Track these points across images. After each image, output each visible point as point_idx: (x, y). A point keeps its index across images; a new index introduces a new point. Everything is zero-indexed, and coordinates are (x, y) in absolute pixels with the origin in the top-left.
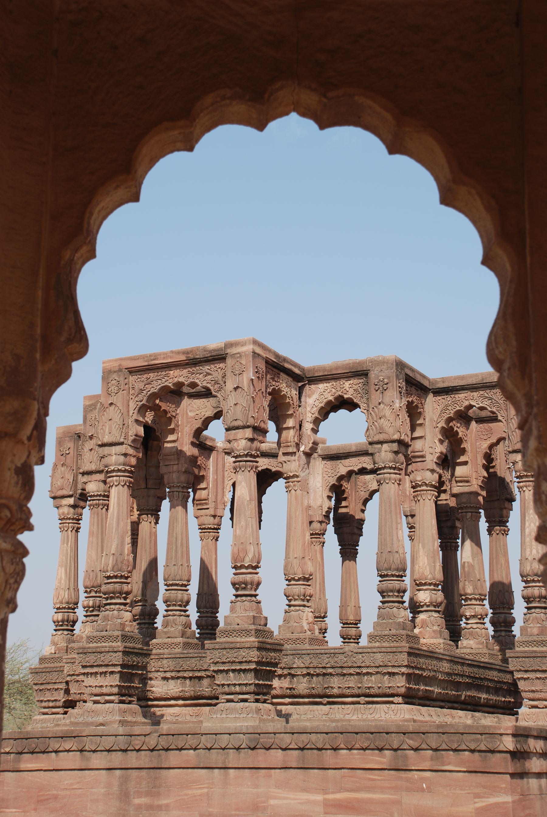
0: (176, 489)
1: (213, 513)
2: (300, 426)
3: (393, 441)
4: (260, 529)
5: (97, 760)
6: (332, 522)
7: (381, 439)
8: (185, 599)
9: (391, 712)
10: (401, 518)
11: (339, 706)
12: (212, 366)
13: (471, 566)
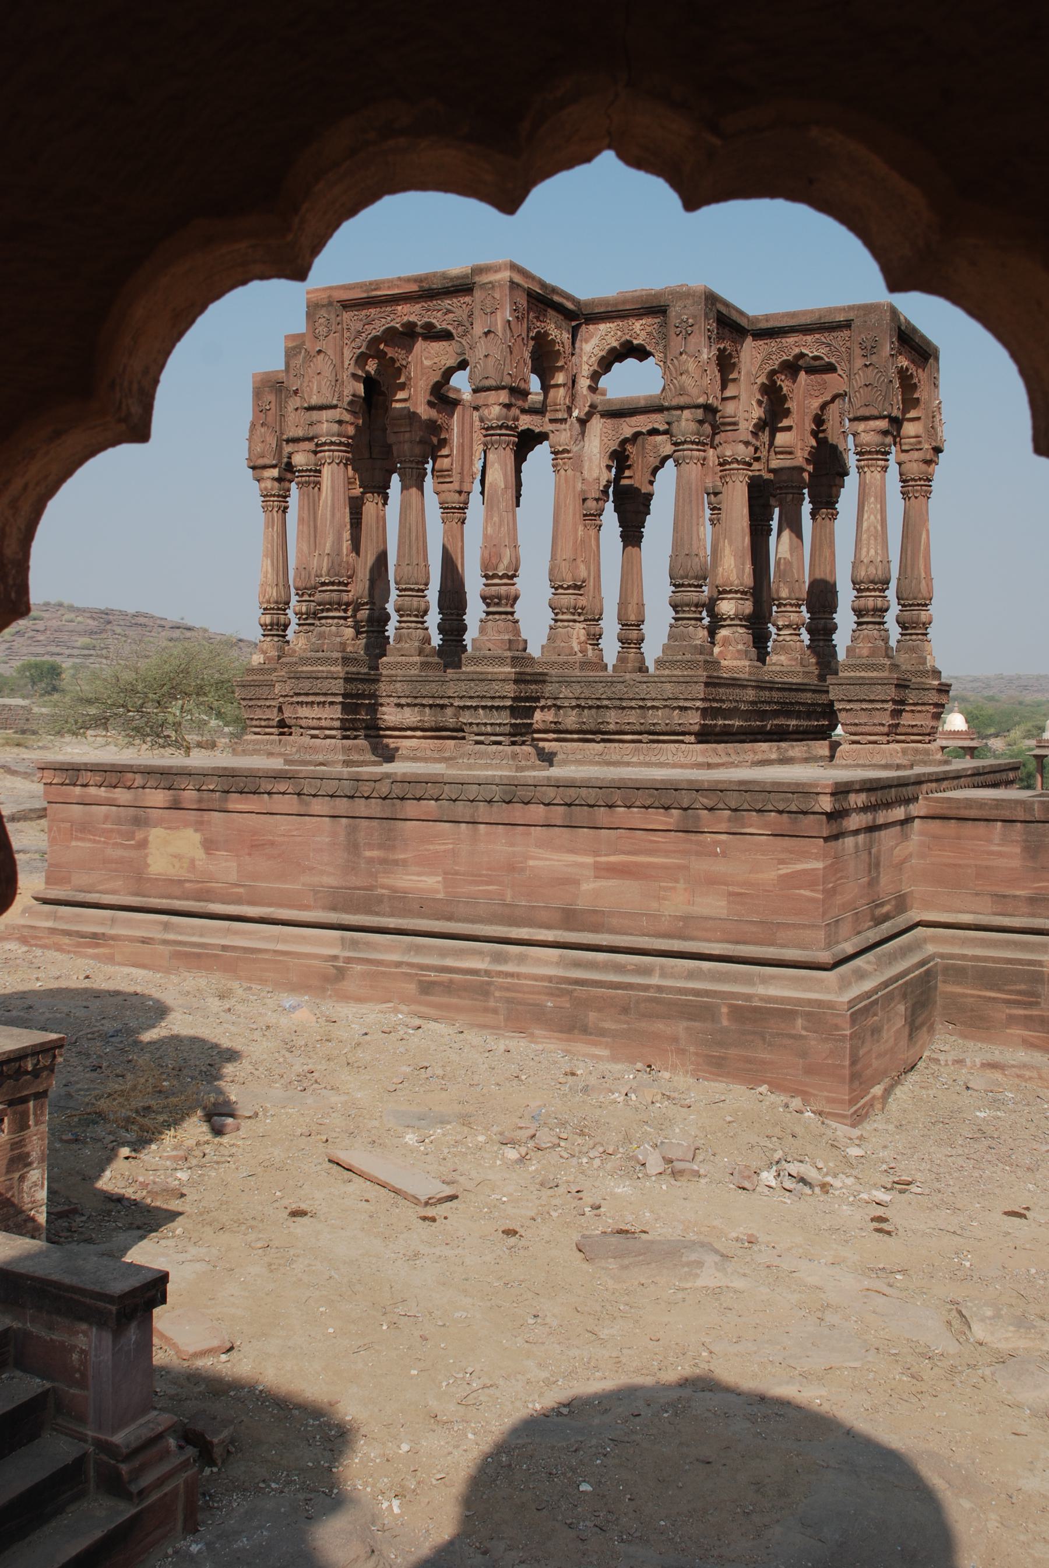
0: (408, 465)
1: (458, 489)
2: (574, 382)
3: (697, 407)
4: (518, 505)
5: (318, 806)
6: (611, 498)
7: (682, 404)
8: (423, 606)
9: (680, 754)
10: (703, 510)
11: (616, 745)
12: (455, 300)
13: (789, 563)
